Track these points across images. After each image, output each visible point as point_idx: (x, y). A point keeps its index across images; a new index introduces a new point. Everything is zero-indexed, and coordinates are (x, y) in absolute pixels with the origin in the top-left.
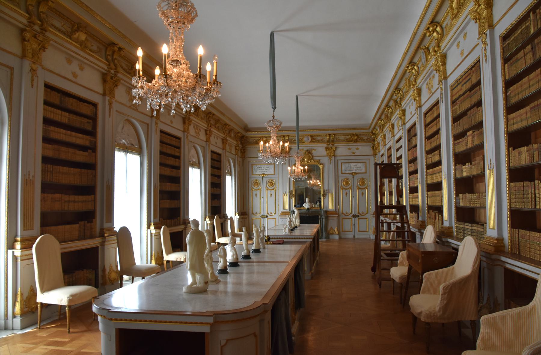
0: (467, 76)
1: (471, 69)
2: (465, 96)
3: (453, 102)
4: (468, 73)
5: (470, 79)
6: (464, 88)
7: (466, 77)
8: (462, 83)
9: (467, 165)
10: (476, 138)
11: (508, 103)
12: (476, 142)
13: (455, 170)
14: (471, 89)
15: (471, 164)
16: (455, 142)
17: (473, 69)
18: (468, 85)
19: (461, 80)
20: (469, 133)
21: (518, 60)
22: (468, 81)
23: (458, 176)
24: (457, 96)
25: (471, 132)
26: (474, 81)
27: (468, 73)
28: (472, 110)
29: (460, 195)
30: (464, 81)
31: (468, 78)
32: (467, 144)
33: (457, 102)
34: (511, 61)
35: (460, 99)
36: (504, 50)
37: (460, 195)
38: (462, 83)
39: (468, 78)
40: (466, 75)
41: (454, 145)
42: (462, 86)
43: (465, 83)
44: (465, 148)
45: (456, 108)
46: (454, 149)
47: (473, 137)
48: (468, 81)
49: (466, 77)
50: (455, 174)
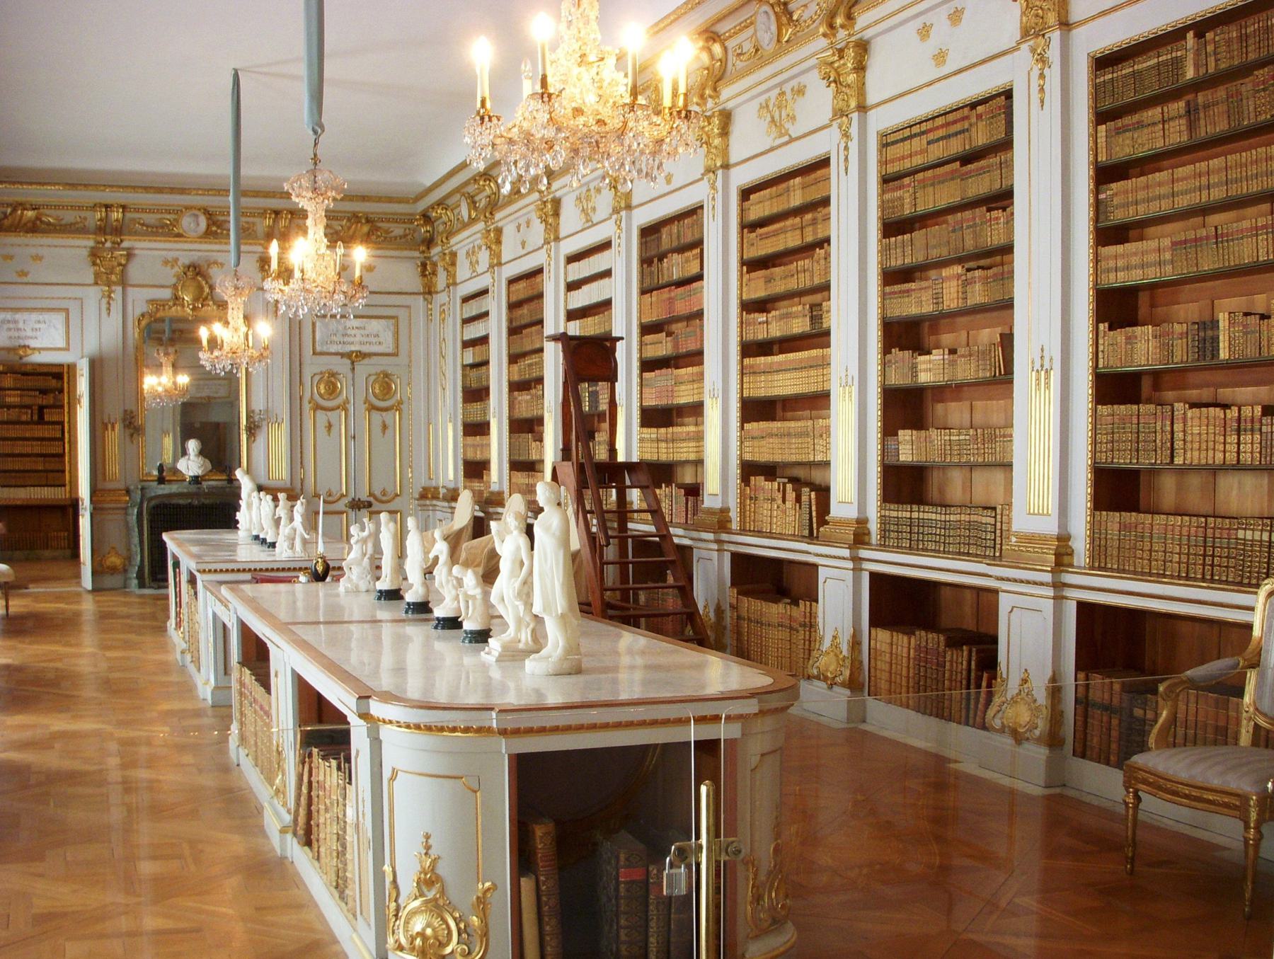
0: (955, 122)
1: (973, 106)
2: (939, 171)
3: (887, 180)
4: (958, 115)
5: (963, 132)
6: (937, 152)
7: (947, 124)
8: (931, 136)
9: (936, 356)
10: (978, 287)
11: (1102, 217)
12: (978, 295)
13: (884, 364)
14: (967, 159)
15: (953, 351)
16: (888, 289)
17: (980, 109)
18: (956, 146)
19: (924, 127)
20: (946, 272)
21: (1140, 125)
22: (956, 134)
23: (895, 380)
24: (907, 164)
25: (958, 269)
26: (981, 138)
27: (958, 115)
28: (968, 214)
29: (901, 432)
30: (941, 133)
31: (958, 127)
32: (938, 298)
33: (907, 181)
34: (1119, 123)
35: (920, 176)
36: (1097, 92)
37: (901, 432)
38: (931, 136)
39: (958, 127)
40: (950, 117)
41: (884, 296)
42: (929, 143)
43: (942, 138)
44: (928, 308)
45: (901, 198)
46: (883, 307)
47: (966, 283)
48: (956, 134)
49: (947, 124)
50: (884, 373)
